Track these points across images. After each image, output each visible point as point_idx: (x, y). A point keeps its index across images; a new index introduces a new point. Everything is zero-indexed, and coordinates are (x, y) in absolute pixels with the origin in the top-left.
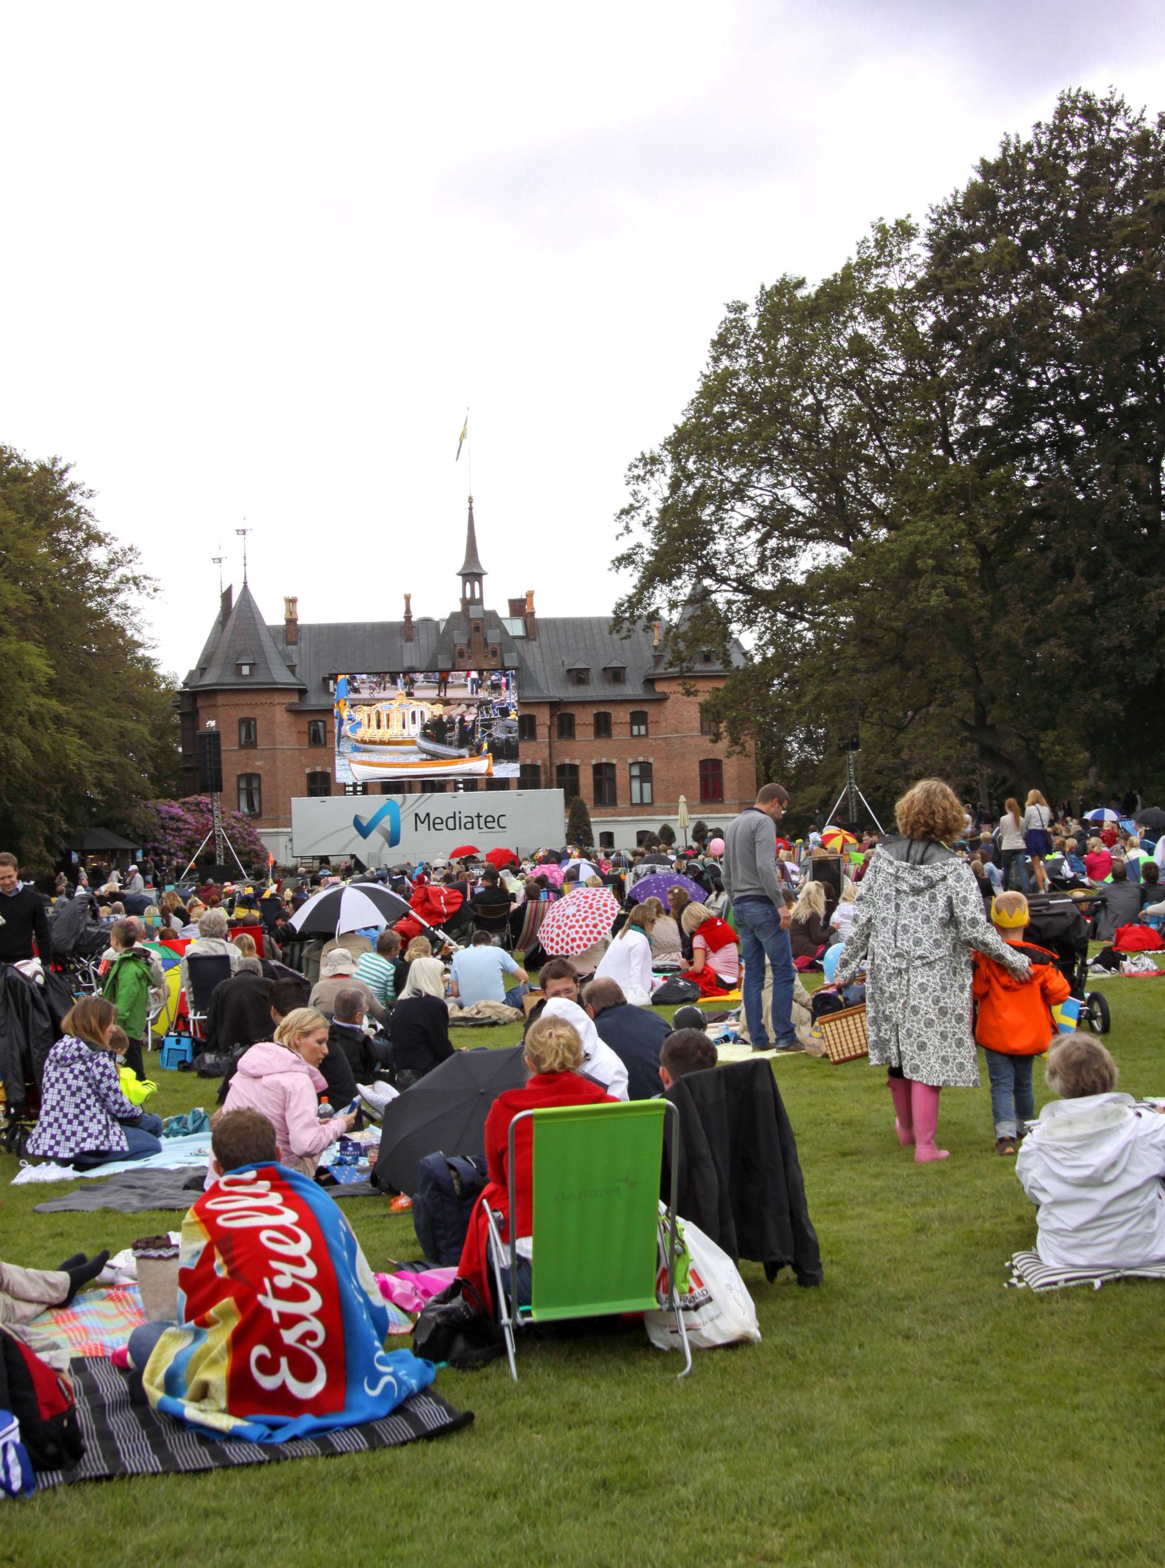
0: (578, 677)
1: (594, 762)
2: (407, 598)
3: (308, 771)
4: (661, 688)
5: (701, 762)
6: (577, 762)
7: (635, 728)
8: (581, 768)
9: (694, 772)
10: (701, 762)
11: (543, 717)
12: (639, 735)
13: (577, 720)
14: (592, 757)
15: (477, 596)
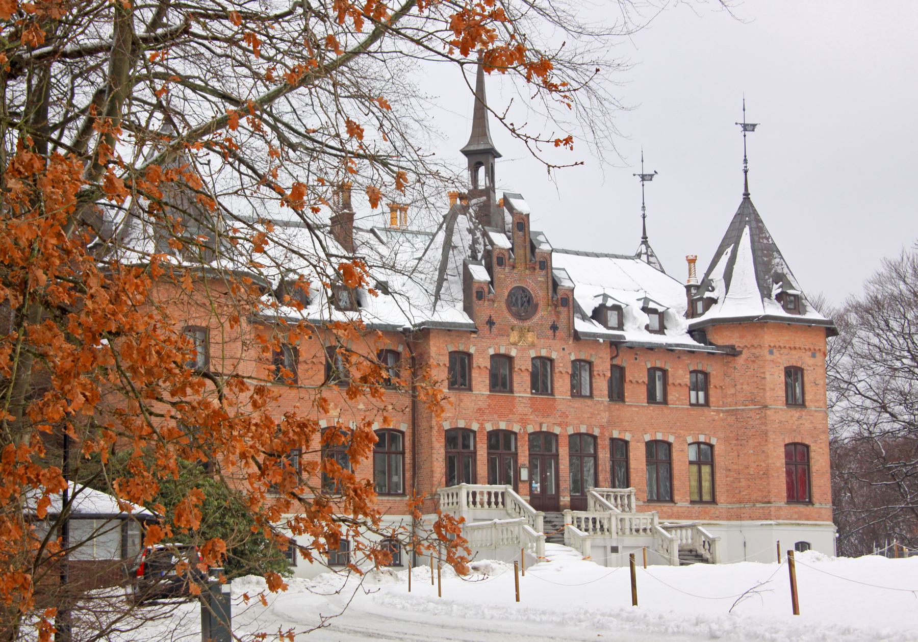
1: (647, 438)
4: (723, 339)
5: (786, 445)
6: (627, 437)
7: (693, 393)
8: (632, 446)
9: (778, 459)
10: (786, 445)
12: (697, 405)
14: (645, 432)
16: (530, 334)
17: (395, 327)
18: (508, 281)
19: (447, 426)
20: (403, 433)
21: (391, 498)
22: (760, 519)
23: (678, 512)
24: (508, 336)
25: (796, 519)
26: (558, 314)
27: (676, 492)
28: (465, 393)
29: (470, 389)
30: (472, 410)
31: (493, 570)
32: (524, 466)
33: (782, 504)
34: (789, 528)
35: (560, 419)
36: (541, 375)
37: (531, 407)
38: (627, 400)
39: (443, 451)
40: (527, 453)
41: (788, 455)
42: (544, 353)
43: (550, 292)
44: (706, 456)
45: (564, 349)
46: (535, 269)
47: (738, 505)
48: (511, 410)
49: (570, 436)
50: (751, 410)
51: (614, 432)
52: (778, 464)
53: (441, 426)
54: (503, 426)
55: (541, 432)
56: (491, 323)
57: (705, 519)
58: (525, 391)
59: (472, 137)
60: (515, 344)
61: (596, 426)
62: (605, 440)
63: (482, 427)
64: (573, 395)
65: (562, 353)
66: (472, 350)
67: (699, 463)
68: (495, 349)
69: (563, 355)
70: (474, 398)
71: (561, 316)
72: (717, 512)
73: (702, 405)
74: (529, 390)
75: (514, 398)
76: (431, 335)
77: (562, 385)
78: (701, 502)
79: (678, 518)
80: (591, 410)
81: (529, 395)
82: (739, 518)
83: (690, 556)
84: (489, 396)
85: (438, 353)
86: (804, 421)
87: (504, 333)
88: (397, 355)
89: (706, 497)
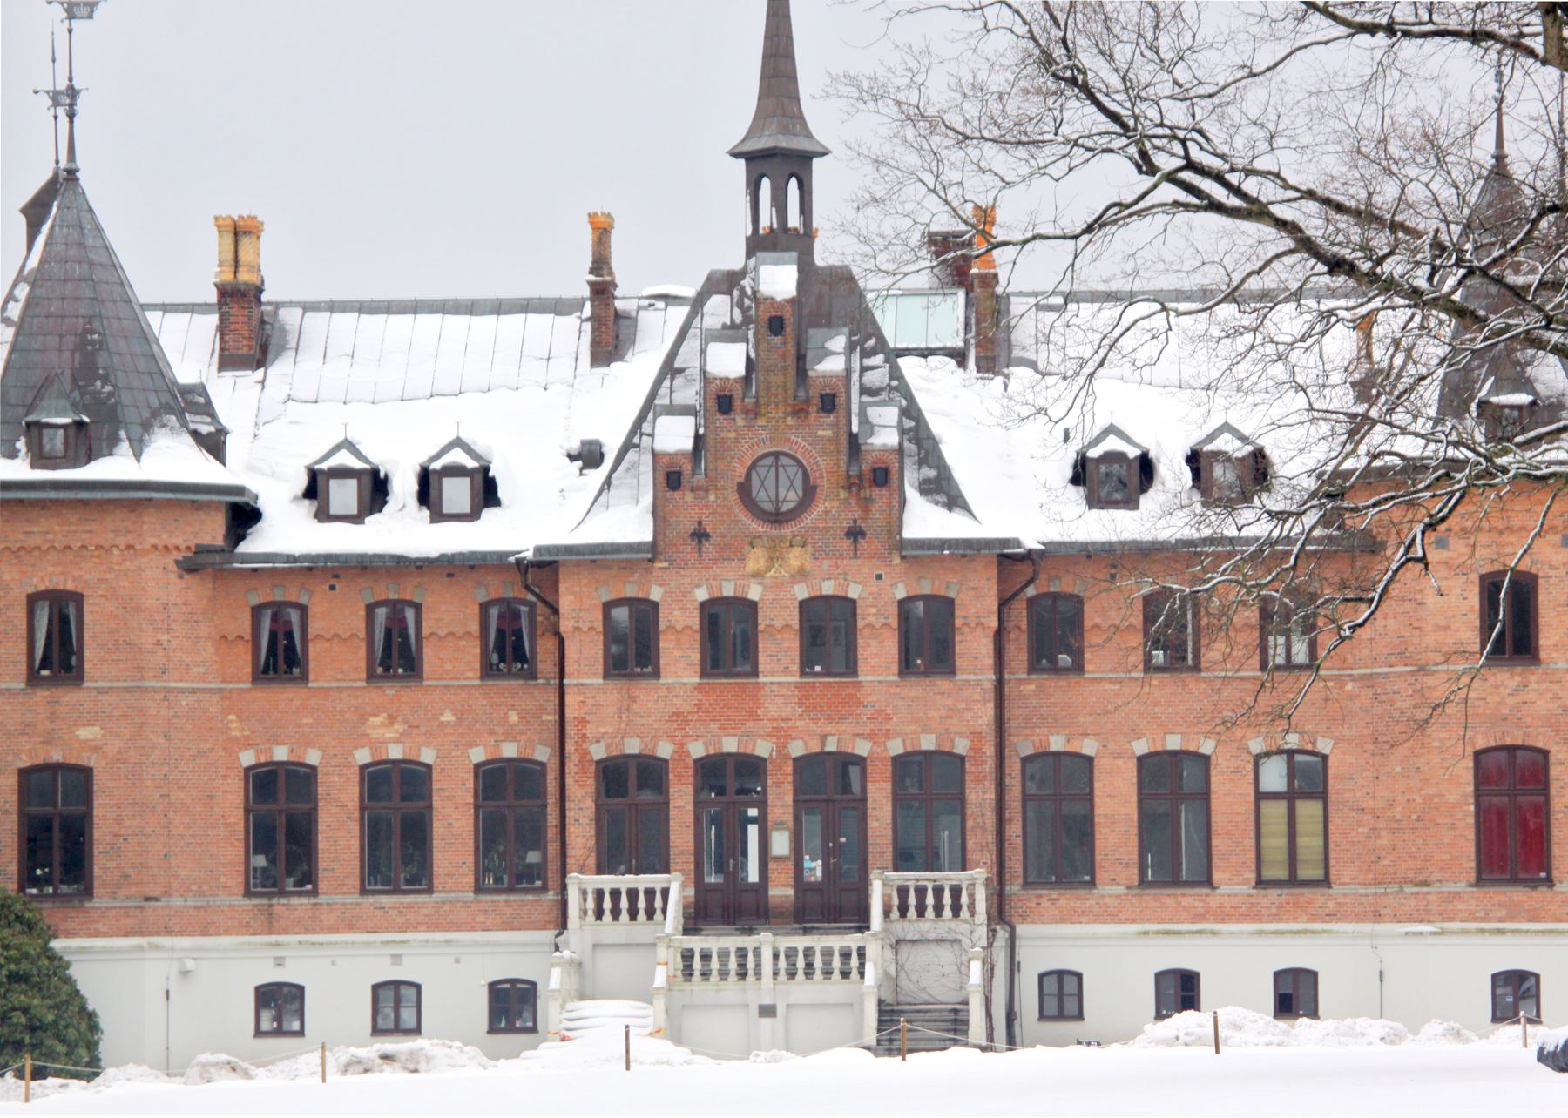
0: (1113, 477)
1: (1141, 747)
2: (602, 232)
3: (248, 758)
5: (1478, 755)
6: (1088, 747)
8: (1100, 766)
9: (1457, 788)
11: (976, 603)
12: (1289, 666)
13: (1091, 616)
15: (794, 220)
16: (796, 551)
17: (503, 555)
18: (745, 444)
19: (598, 752)
20: (542, 764)
21: (512, 898)
22: (1410, 920)
23: (1221, 906)
24: (743, 559)
25: (1501, 920)
26: (866, 505)
27: (1216, 862)
28: (643, 683)
29: (656, 674)
30: (668, 720)
31: (429, 1059)
32: (780, 825)
33: (1461, 887)
34: (1527, 940)
35: (871, 725)
36: (827, 633)
37: (800, 704)
38: (1088, 667)
39: (589, 804)
40: (789, 799)
41: (1483, 777)
42: (828, 588)
43: (844, 458)
44: (1309, 780)
45: (879, 577)
46: (807, 413)
47: (1372, 890)
48: (751, 713)
49: (896, 760)
50: (1399, 675)
51: (1053, 739)
52: (1452, 797)
53: (584, 754)
54: (730, 745)
55: (823, 755)
56: (700, 535)
57: (1295, 920)
58: (786, 671)
59: (755, 119)
60: (757, 575)
61: (962, 736)
62: (983, 762)
63: (681, 751)
64: (901, 673)
65: (874, 585)
66: (656, 594)
67: (1290, 797)
68: (710, 588)
69: (877, 593)
70: (663, 692)
71: (875, 509)
72: (1331, 904)
73: (1300, 667)
74: (796, 668)
75: (760, 686)
76: (563, 573)
77: (878, 652)
78: (1293, 881)
79: (1223, 921)
80: (949, 702)
81: (796, 679)
82: (1377, 917)
83: (900, 1027)
84: (698, 687)
85: (580, 608)
86: (1533, 696)
87: (732, 552)
88: (532, 606)
89: (1304, 873)
